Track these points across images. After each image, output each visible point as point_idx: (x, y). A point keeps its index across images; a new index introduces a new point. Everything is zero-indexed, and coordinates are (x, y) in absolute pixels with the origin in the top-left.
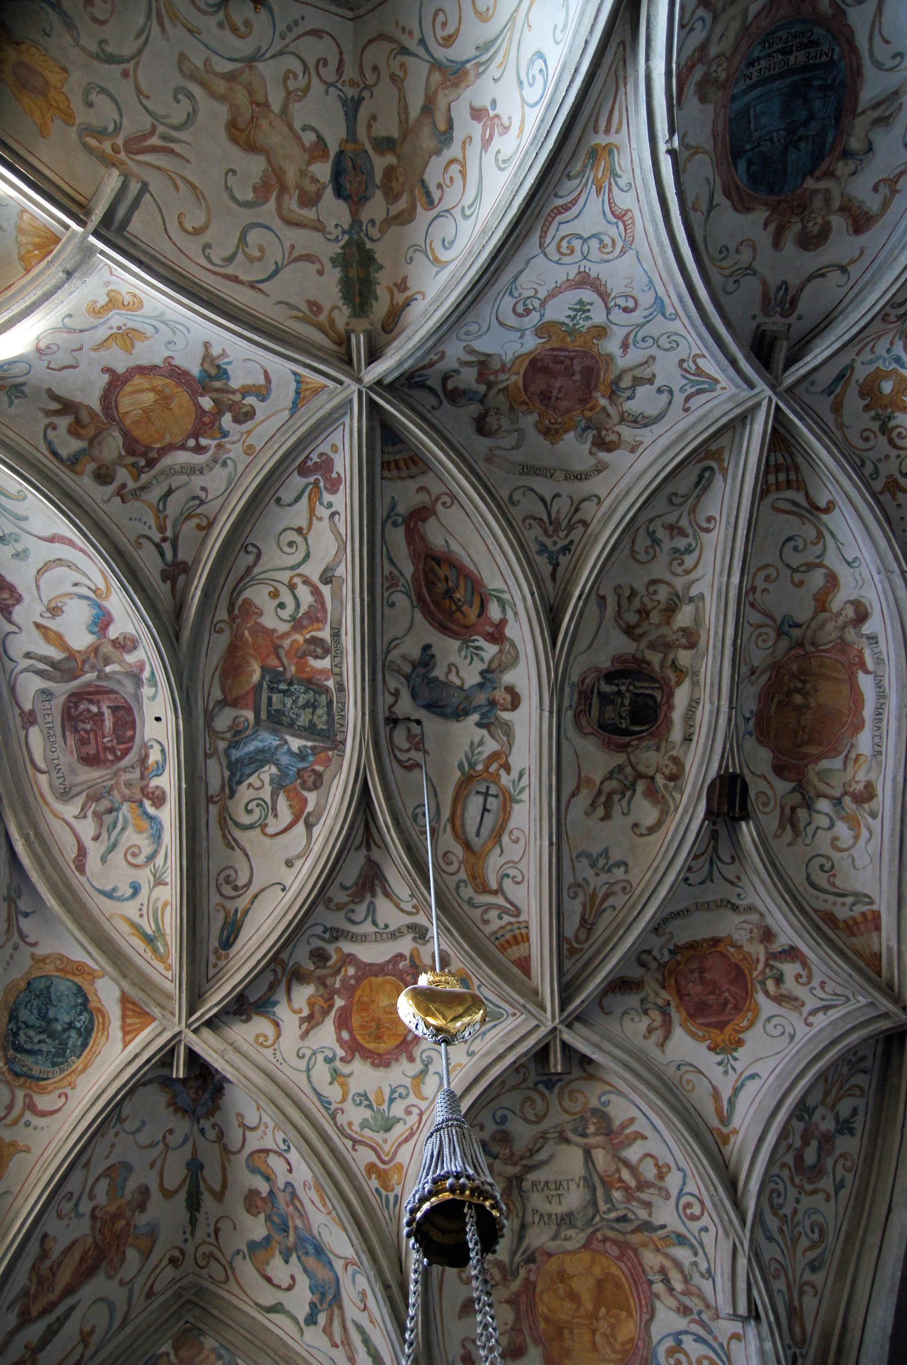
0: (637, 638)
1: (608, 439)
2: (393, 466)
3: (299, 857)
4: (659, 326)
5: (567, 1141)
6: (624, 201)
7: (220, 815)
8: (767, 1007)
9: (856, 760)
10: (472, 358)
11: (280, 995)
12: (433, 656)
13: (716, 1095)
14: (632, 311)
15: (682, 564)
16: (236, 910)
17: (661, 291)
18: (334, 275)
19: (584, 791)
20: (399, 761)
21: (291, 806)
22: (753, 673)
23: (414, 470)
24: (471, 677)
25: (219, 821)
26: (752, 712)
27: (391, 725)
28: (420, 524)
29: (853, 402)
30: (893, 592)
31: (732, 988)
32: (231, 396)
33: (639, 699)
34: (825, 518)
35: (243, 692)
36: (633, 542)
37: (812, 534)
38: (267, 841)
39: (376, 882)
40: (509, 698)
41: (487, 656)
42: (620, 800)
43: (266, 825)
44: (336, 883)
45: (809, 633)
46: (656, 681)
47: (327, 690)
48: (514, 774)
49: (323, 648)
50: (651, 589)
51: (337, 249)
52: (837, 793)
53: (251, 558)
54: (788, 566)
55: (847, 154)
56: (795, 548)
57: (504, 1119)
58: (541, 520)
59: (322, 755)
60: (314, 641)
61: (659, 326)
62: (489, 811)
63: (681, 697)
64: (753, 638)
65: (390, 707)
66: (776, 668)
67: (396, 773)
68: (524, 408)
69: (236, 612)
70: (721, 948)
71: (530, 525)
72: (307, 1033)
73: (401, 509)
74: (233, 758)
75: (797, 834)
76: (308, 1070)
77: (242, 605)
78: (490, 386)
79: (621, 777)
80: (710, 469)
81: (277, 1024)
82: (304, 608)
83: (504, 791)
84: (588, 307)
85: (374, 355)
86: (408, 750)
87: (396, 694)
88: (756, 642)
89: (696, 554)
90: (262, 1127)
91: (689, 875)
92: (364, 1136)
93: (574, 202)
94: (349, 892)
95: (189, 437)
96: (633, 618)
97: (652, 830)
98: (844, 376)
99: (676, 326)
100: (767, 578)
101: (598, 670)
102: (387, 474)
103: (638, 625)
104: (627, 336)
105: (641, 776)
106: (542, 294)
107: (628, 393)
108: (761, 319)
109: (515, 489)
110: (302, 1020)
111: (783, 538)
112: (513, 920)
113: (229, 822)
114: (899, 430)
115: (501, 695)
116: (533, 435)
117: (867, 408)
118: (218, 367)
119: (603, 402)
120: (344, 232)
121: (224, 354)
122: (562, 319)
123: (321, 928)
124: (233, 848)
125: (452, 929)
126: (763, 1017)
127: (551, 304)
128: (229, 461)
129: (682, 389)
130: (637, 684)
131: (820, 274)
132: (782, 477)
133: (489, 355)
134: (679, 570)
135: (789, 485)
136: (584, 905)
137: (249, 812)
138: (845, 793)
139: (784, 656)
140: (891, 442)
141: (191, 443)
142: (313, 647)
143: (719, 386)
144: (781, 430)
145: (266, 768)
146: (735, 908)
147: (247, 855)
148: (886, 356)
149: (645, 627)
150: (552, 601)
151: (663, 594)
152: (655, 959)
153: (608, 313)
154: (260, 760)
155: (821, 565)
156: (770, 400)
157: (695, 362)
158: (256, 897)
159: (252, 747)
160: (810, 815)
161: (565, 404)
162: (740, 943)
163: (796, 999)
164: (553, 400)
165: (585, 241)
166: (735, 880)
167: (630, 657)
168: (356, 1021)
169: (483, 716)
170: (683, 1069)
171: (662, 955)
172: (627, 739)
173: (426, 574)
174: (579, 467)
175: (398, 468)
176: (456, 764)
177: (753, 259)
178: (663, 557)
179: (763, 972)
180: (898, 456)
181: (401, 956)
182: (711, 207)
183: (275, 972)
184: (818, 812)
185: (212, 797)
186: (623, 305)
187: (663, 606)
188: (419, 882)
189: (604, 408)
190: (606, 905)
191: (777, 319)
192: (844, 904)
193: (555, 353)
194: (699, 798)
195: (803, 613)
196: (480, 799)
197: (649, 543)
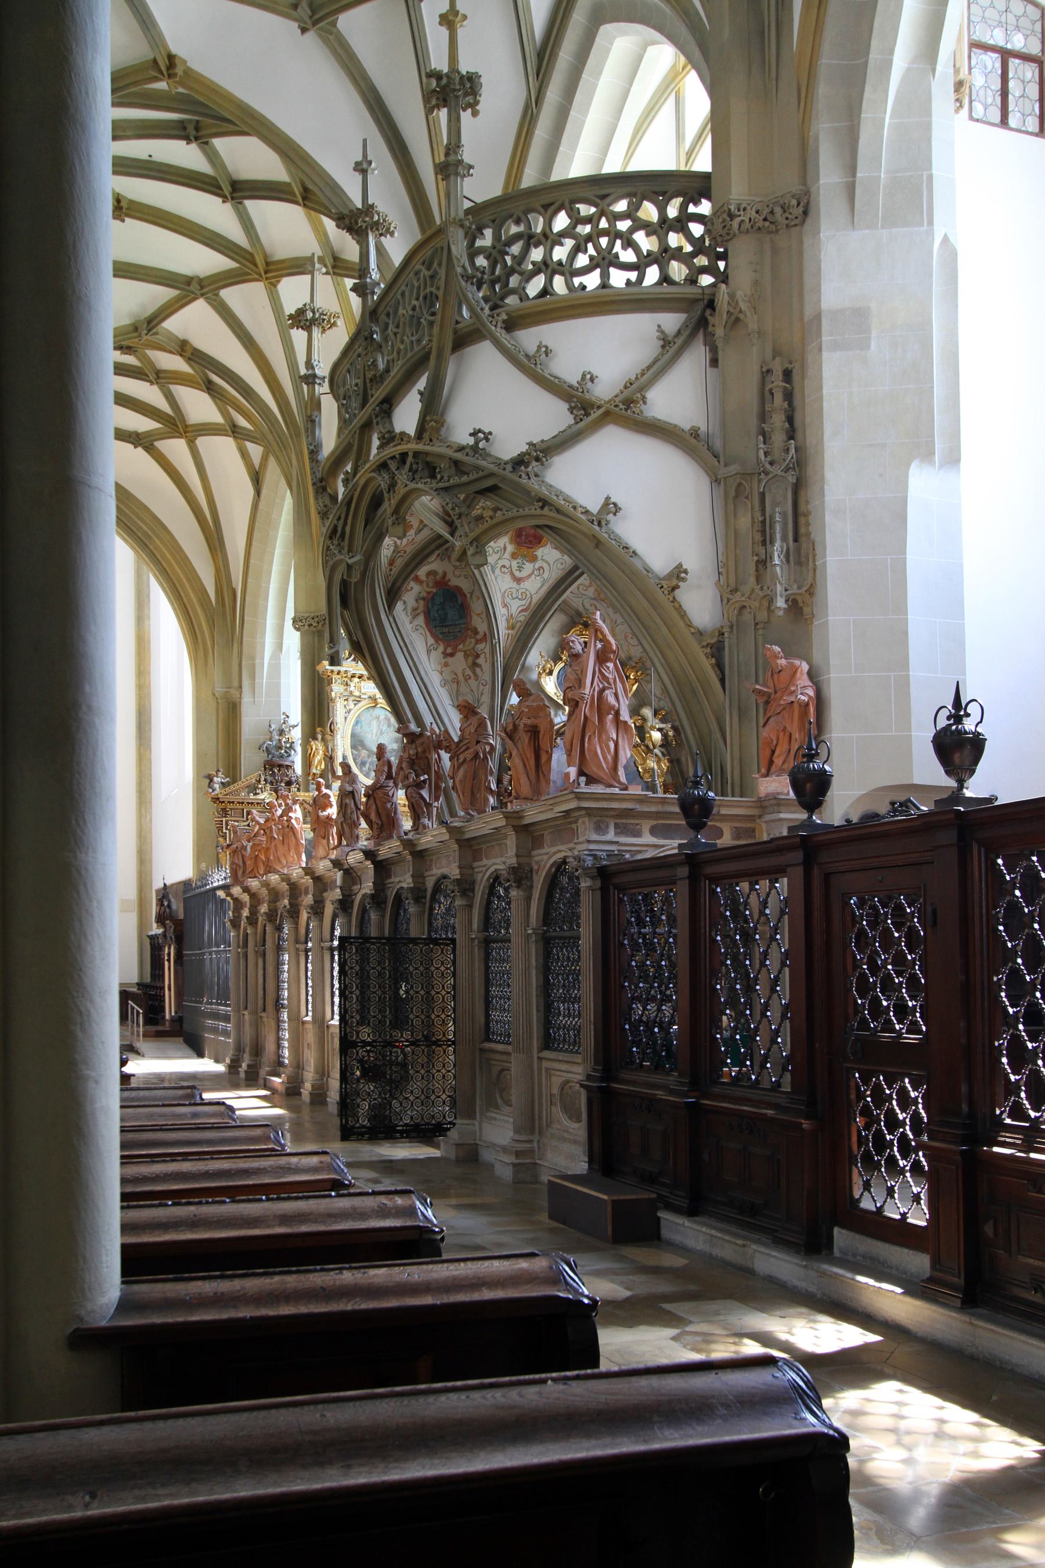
6: (504, 611)
55: (423, 599)
93: (520, 612)
106: (533, 576)
122: (527, 563)
127: (531, 571)
165: (517, 597)
182: (471, 594)
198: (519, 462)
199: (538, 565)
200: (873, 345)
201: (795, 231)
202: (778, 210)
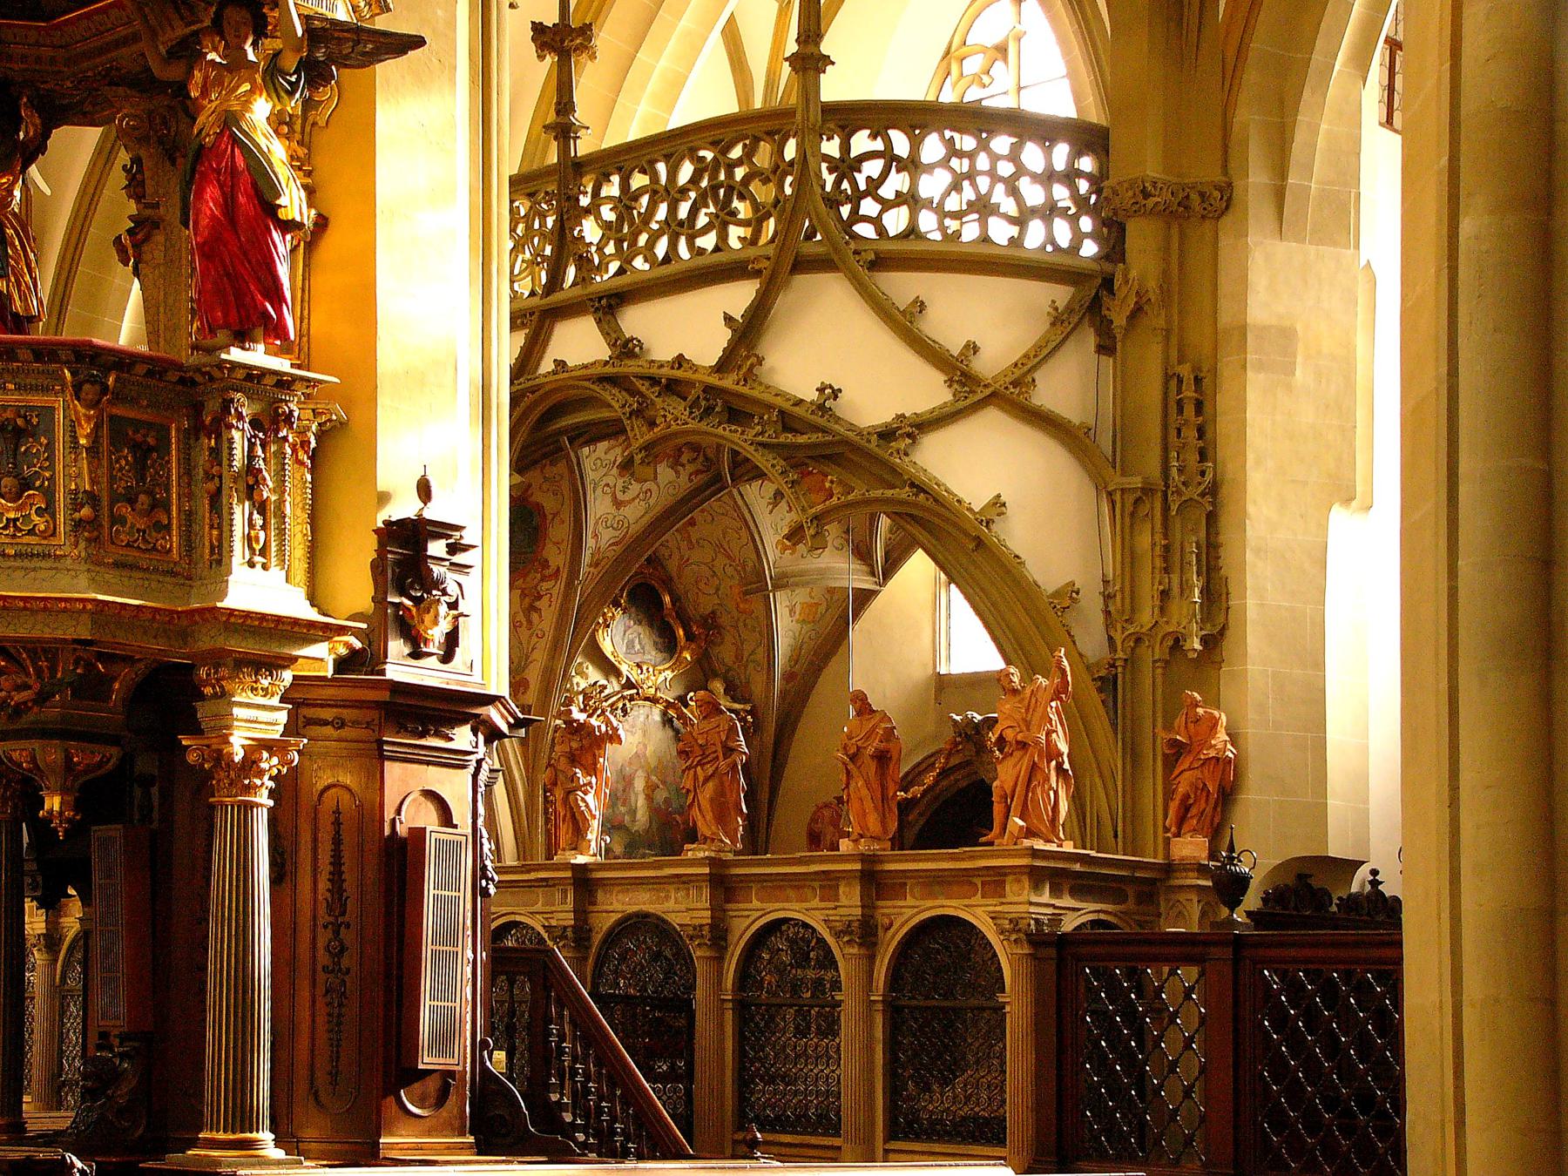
182: (555, 515)
198: (887, 434)
200: (1298, 373)
201: (1208, 224)
202: (1195, 197)
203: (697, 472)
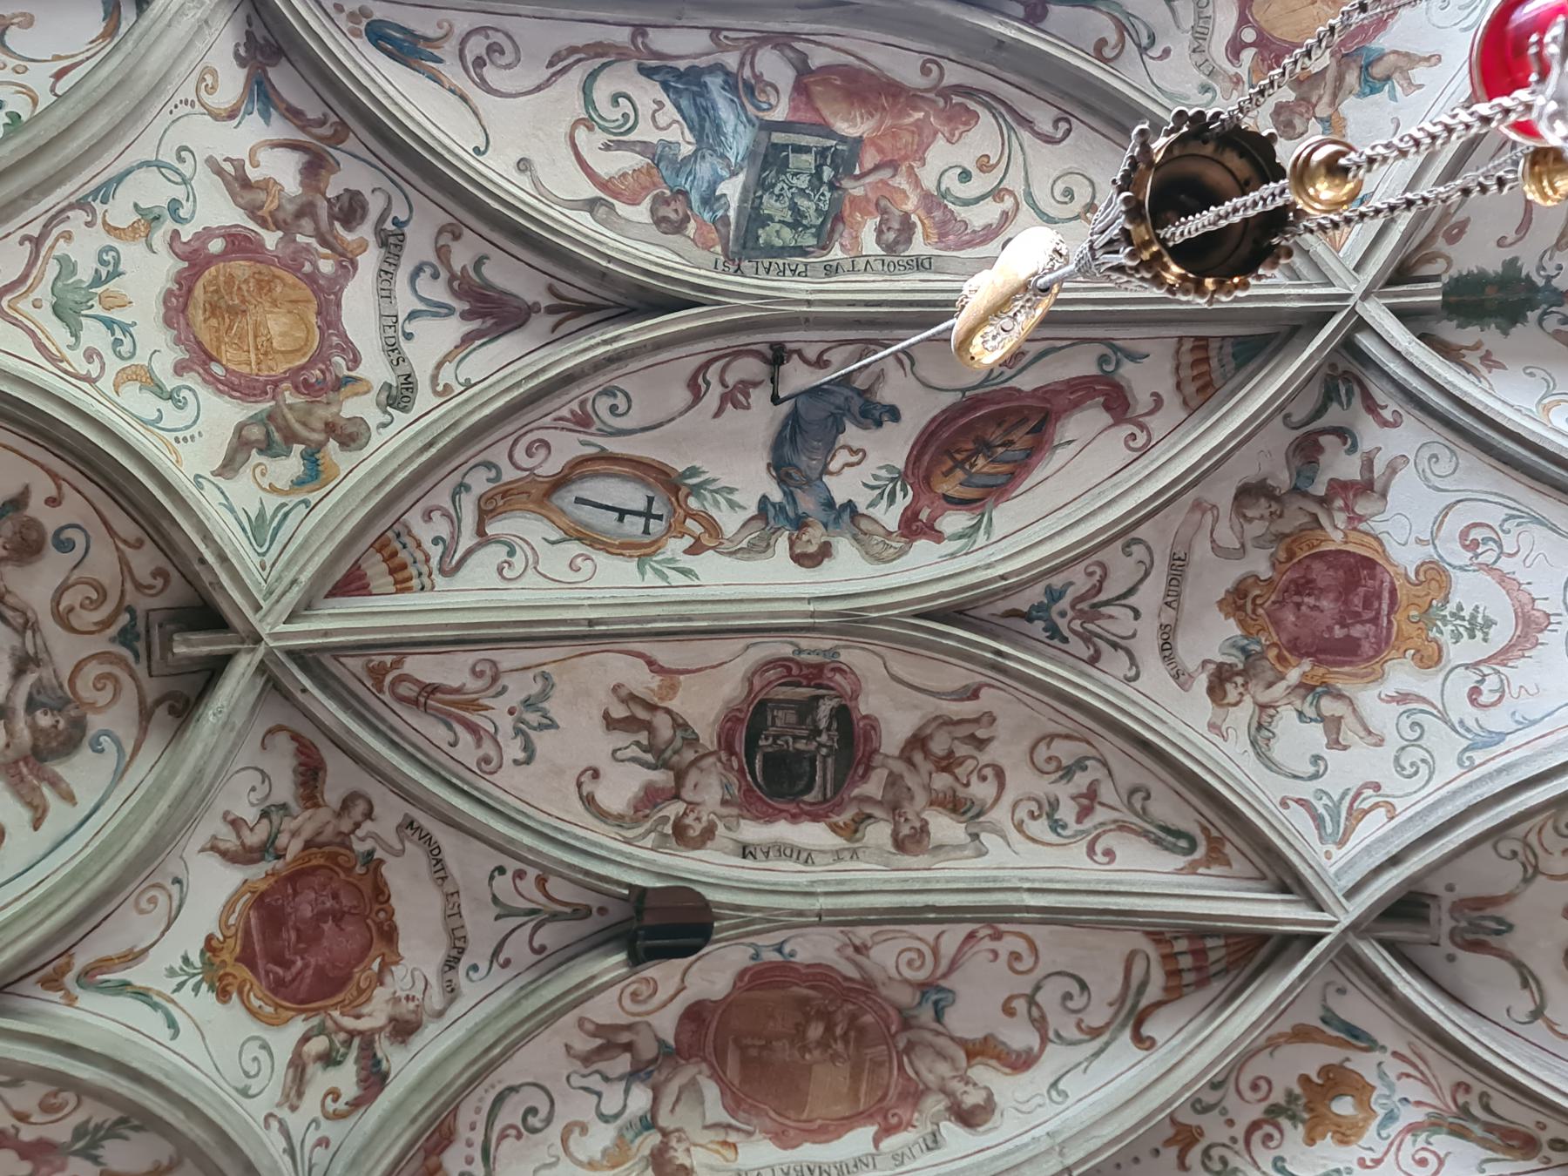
0: (906, 755)
1: (1229, 687)
2: (1200, 355)
3: (536, 183)
4: (1444, 745)
5: (19, 672)
7: (611, 46)
8: (285, 1040)
9: (725, 1143)
10: (1379, 468)
11: (281, 129)
12: (879, 424)
13: (132, 957)
14: (1473, 702)
15: (1033, 816)
16: (440, 61)
17: (1513, 740)
18: (1491, 262)
19: (655, 681)
20: (706, 366)
21: (624, 175)
22: (857, 949)
23: (1190, 389)
24: (845, 485)
25: (600, 44)
26: (792, 954)
27: (769, 354)
28: (1101, 399)
29: (1311, 1059)
30: (1029, 1161)
31: (309, 972)
32: (1326, 99)
33: (806, 766)
34: (1127, 1035)
35: (819, 104)
36: (1068, 737)
37: (1096, 1018)
38: (564, 128)
39: (490, 322)
40: (812, 549)
41: (878, 512)
42: (638, 743)
43: (590, 129)
44: (488, 249)
45: (929, 1036)
46: (836, 790)
47: (825, 247)
48: (688, 562)
49: (896, 242)
50: (988, 772)
51: (1528, 268)
52: (664, 1120)
53: (1046, 127)
54: (1038, 988)
56: (1068, 996)
57: (64, 546)
58: (1100, 591)
59: (714, 235)
60: (907, 228)
61: (1444, 745)
62: (621, 519)
63: (813, 834)
64: (917, 944)
65: (799, 352)
66: (867, 988)
67: (687, 360)
68: (1282, 555)
69: (956, 99)
70: (378, 946)
71: (1091, 574)
72: (219, 172)
73: (1128, 371)
74: (708, 79)
75: (587, 1059)
76: (159, 165)
77: (967, 109)
78: (1324, 501)
79: (678, 743)
80: (1193, 847)
81: (232, 115)
82: (962, 212)
83: (656, 545)
84: (1479, 635)
85: (1403, 315)
86: (723, 384)
87: (820, 363)
88: (909, 949)
89: (1052, 838)
90: (12, 62)
91: (509, 874)
92: (46, 262)
94: (472, 273)
95: (1260, 32)
96: (939, 746)
97: (589, 801)
98: (1356, 1037)
99: (1448, 769)
100: (1015, 956)
101: (855, 696)
102: (1188, 345)
103: (927, 754)
104: (1424, 700)
105: (680, 776)
106: (1505, 565)
107: (1310, 712)
108: (1447, 899)
109: (1148, 548)
110: (239, 165)
111: (1083, 976)
112: (434, 562)
113: (598, 62)
114: (1277, 1135)
115: (814, 536)
116: (1233, 573)
117: (1305, 1080)
118: (1388, 78)
119: (1294, 675)
120: (1549, 279)
121: (1411, 86)
123: (402, 218)
124: (551, 64)
125: (433, 450)
126: (269, 1035)
128: (1209, 95)
129: (1321, 793)
130: (830, 760)
131: (1527, 978)
132: (1186, 962)
133: (1384, 495)
134: (1022, 813)
135: (1173, 973)
136: (458, 691)
137: (615, 103)
138: (665, 1134)
139: (885, 999)
140: (1255, 1126)
141: (1249, 35)
142: (896, 226)
143: (1332, 848)
144: (1264, 952)
145: (689, 137)
146: (451, 963)
147: (539, 88)
148: (1396, 1098)
149: (925, 766)
150: (971, 613)
151: (982, 790)
152: (358, 825)
153: (1467, 667)
154: (702, 127)
155: (1044, 1040)
156: (1331, 924)
157: (1377, 805)
158: (464, 98)
159: (726, 112)
160: (620, 1078)
161: (1290, 617)
162: (388, 979)
163: (300, 1094)
164: (1297, 599)
166: (501, 959)
167: (875, 745)
168: (241, 268)
169: (780, 508)
170: (175, 889)
171: (362, 840)
172: (740, 747)
173: (1019, 410)
174: (1182, 645)
175: (1195, 364)
176: (697, 464)
177: (1552, 877)
178: (1043, 787)
179: (340, 1028)
180: (1234, 1140)
181: (356, 361)
183: (322, 123)
184: (627, 1092)
185: (644, 35)
186: (1484, 688)
187: (962, 792)
188: (515, 393)
189: (1281, 677)
190: (459, 728)
191: (1447, 924)
192: (469, 1161)
193: (1386, 595)
194: (659, 875)
195: (965, 1020)
196: (641, 505)
197: (1065, 762)
199: (1455, 554)
203: (1372, 407)
